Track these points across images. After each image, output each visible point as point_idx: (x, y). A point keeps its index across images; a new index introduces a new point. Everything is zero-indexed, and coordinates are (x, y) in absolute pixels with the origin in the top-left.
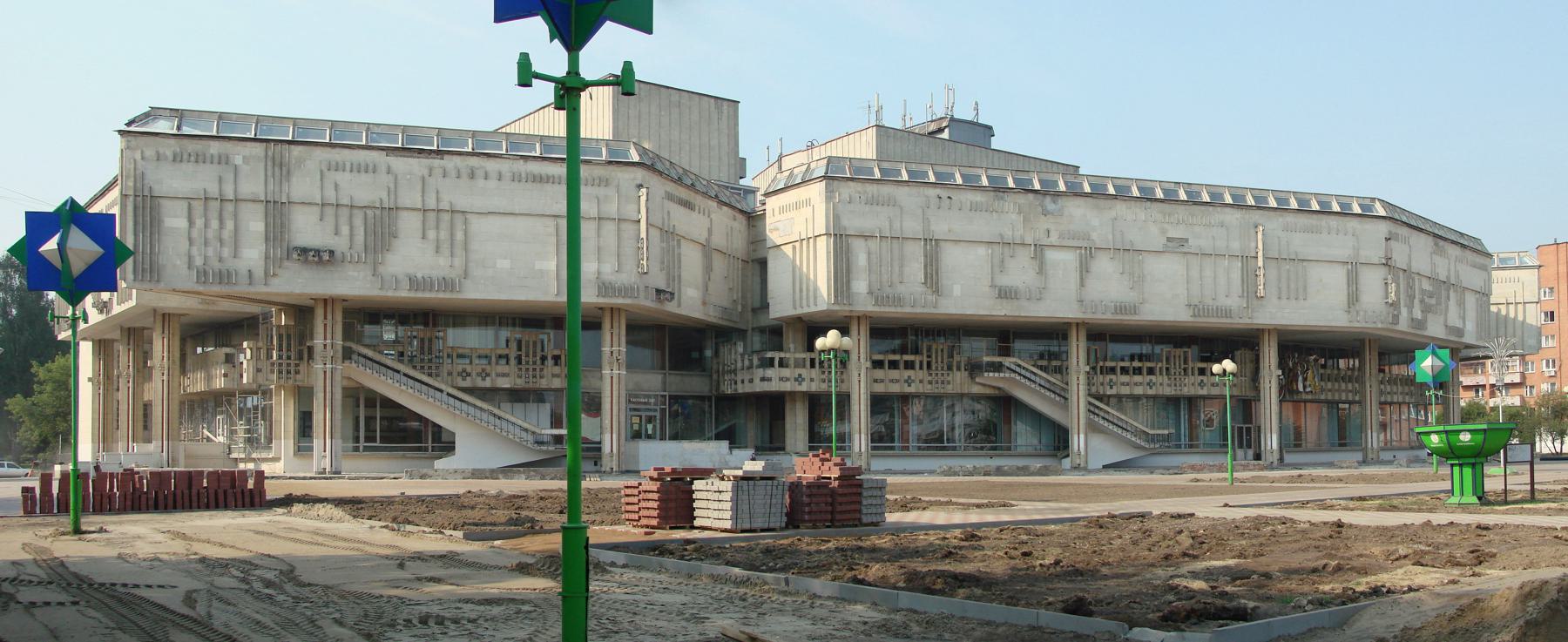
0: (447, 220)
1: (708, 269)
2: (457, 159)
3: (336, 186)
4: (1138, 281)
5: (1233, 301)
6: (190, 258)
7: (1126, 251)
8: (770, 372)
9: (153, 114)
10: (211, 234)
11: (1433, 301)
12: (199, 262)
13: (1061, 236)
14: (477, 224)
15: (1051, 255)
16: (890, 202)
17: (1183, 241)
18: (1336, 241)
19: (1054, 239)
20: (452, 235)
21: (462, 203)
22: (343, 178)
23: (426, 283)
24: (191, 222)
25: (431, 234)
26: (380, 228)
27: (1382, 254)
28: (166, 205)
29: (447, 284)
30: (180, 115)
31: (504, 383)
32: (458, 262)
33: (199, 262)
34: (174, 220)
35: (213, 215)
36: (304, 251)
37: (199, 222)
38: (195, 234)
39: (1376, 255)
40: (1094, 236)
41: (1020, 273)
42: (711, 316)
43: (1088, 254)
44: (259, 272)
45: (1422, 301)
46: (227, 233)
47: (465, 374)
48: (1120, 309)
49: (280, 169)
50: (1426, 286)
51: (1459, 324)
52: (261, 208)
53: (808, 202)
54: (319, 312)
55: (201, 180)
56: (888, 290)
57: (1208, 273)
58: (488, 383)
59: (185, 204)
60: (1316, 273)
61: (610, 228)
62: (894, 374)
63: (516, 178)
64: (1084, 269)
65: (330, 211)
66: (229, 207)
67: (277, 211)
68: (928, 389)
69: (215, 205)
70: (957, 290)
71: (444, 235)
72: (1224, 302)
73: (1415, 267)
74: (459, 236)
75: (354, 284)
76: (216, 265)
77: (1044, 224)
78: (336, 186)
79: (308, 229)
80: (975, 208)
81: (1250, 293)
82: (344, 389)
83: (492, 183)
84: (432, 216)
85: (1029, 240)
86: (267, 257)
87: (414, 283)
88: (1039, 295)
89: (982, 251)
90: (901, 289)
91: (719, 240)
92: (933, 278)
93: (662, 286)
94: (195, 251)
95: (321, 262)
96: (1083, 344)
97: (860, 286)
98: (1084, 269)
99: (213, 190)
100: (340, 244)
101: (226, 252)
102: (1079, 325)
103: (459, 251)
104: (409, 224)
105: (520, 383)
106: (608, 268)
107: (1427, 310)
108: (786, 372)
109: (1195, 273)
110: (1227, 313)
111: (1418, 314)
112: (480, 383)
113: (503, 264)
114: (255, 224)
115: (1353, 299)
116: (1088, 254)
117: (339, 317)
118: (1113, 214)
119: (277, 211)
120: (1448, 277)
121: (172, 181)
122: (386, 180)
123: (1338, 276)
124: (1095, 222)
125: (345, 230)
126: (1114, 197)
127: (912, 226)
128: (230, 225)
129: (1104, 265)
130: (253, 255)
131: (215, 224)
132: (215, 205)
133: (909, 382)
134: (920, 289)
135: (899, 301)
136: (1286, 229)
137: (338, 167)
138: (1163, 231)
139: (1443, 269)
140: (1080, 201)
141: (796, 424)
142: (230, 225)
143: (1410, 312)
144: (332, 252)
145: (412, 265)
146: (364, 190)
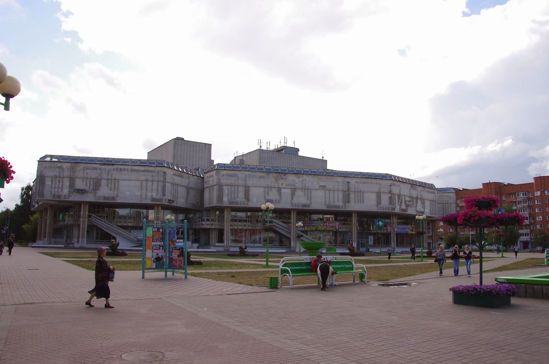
0: (114, 182)
1: (188, 194)
2: (117, 166)
3: (87, 173)
4: (310, 198)
5: (340, 204)
6: (51, 191)
7: (306, 189)
8: (203, 223)
9: (46, 156)
10: (57, 186)
11: (411, 203)
12: (53, 193)
13: (286, 185)
14: (122, 183)
15: (283, 190)
16: (235, 175)
17: (324, 187)
18: (374, 186)
19: (284, 186)
20: (115, 186)
21: (118, 177)
22: (89, 171)
23: (108, 198)
24: (52, 182)
25: (110, 185)
26: (97, 185)
27: (389, 190)
28: (47, 179)
29: (113, 198)
30: (52, 157)
31: (130, 225)
32: (116, 193)
33: (53, 193)
34: (48, 182)
35: (57, 181)
36: (78, 190)
37: (54, 183)
38: (53, 186)
39: (387, 190)
40: (296, 185)
41: (273, 195)
42: (189, 206)
43: (294, 191)
44: (67, 196)
45: (406, 203)
46: (60, 186)
47: (120, 222)
48: (304, 205)
49: (72, 169)
50: (407, 199)
51: (422, 210)
52: (68, 179)
53: (213, 176)
54: (82, 205)
55: (56, 173)
56: (234, 200)
57: (332, 195)
58: (126, 224)
59: (140, 182)
60: (366, 195)
61: (155, 184)
62: (240, 223)
63: (132, 170)
64: (293, 194)
65: (85, 180)
66: (61, 179)
67: (72, 180)
68: (251, 228)
69: (110, 181)
70: (255, 200)
71: (113, 186)
72: (337, 204)
73: (402, 193)
74: (117, 186)
75: (89, 198)
76: (57, 194)
77: (281, 182)
78: (87, 173)
79: (79, 184)
80: (260, 177)
81: (347, 199)
82: (88, 225)
83: (126, 172)
84: (110, 181)
85: (276, 186)
86: (69, 191)
87: (105, 198)
88: (279, 201)
89: (262, 189)
90: (238, 200)
91: (191, 185)
92: (247, 196)
93: (171, 198)
94: (53, 190)
95: (82, 193)
96: (295, 215)
97: (225, 199)
98: (293, 194)
99: (58, 174)
100: (87, 188)
101: (60, 190)
102: (294, 210)
103: (116, 190)
104: (104, 183)
105: (134, 225)
106: (154, 194)
107: (407, 206)
108: (208, 223)
109: (327, 196)
110: (338, 207)
111: (403, 207)
112: (124, 224)
113: (128, 193)
114: (67, 183)
115: (379, 202)
116: (294, 191)
117: (87, 207)
118: (301, 179)
119: (72, 180)
120: (417, 196)
121: (49, 173)
122: (99, 171)
123: (373, 196)
124: (297, 181)
125: (88, 184)
126: (303, 174)
127: (241, 182)
128: (61, 183)
129: (299, 193)
130: (66, 191)
131: (58, 183)
132: (58, 179)
133: (245, 226)
134: (243, 200)
135: (237, 203)
136: (357, 182)
137: (88, 169)
138: (318, 184)
139: (414, 193)
140: (293, 175)
141: (214, 236)
142: (61, 183)
143: (400, 206)
144: (85, 190)
145: (104, 193)
146: (93, 174)
